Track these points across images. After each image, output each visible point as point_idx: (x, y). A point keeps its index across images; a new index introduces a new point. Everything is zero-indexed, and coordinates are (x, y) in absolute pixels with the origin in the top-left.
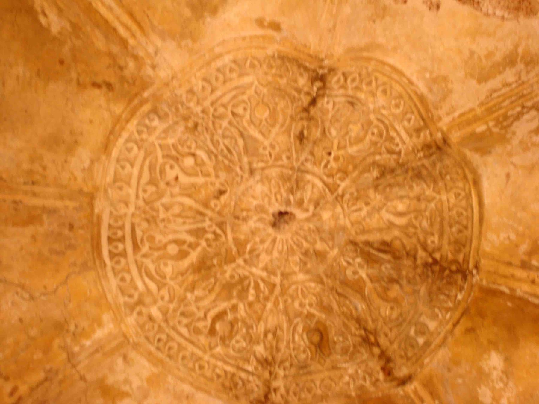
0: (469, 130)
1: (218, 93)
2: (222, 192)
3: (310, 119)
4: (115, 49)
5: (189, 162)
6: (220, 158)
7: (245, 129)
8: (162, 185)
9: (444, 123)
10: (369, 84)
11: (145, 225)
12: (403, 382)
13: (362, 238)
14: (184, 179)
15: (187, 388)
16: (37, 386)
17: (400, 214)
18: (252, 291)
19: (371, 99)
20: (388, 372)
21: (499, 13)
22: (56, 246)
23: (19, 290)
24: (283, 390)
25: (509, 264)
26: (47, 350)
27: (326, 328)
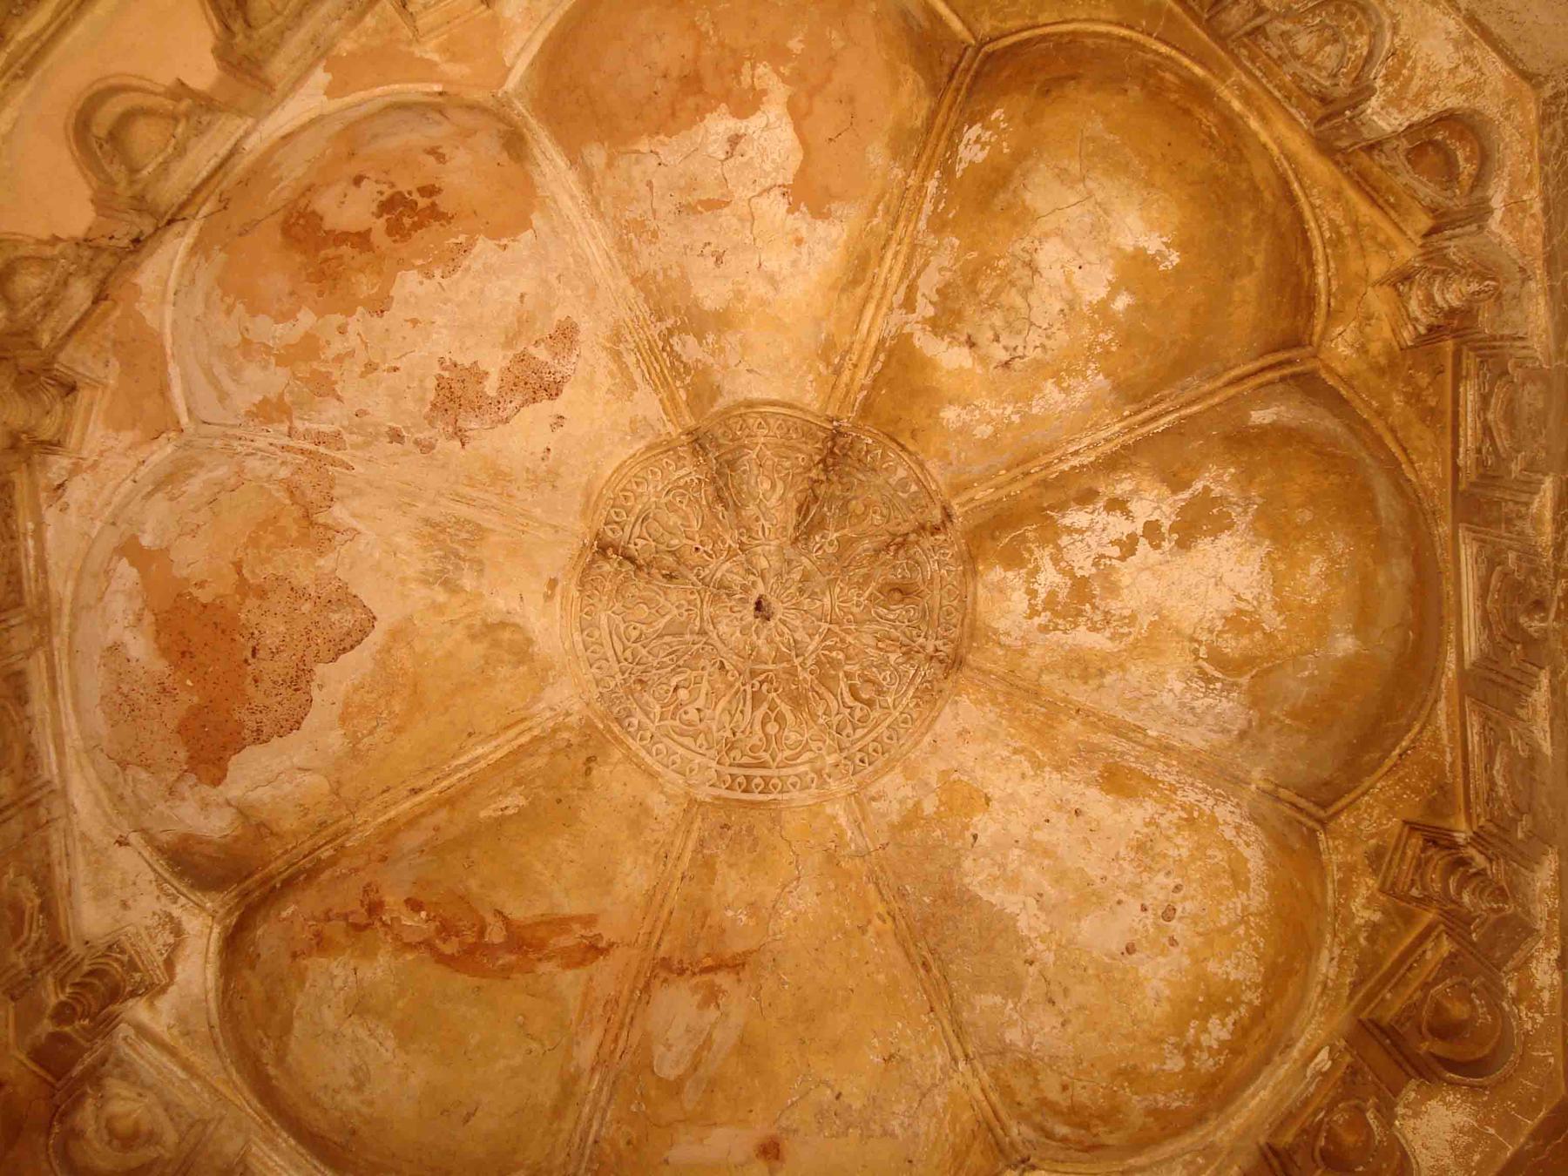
0: (683, 406)
1: (610, 653)
2: (722, 666)
3: (649, 565)
4: (546, 748)
5: (683, 693)
6: (681, 662)
7: (655, 632)
8: (701, 726)
9: (674, 431)
10: (626, 498)
11: (735, 753)
12: (948, 516)
13: (791, 530)
14: (700, 703)
15: (928, 739)
16: (880, 893)
17: (773, 486)
18: (834, 654)
19: (645, 499)
20: (936, 530)
21: (574, 359)
22: (746, 845)
23: (787, 889)
24: (939, 643)
25: (834, 387)
26: (849, 875)
27: (882, 586)
